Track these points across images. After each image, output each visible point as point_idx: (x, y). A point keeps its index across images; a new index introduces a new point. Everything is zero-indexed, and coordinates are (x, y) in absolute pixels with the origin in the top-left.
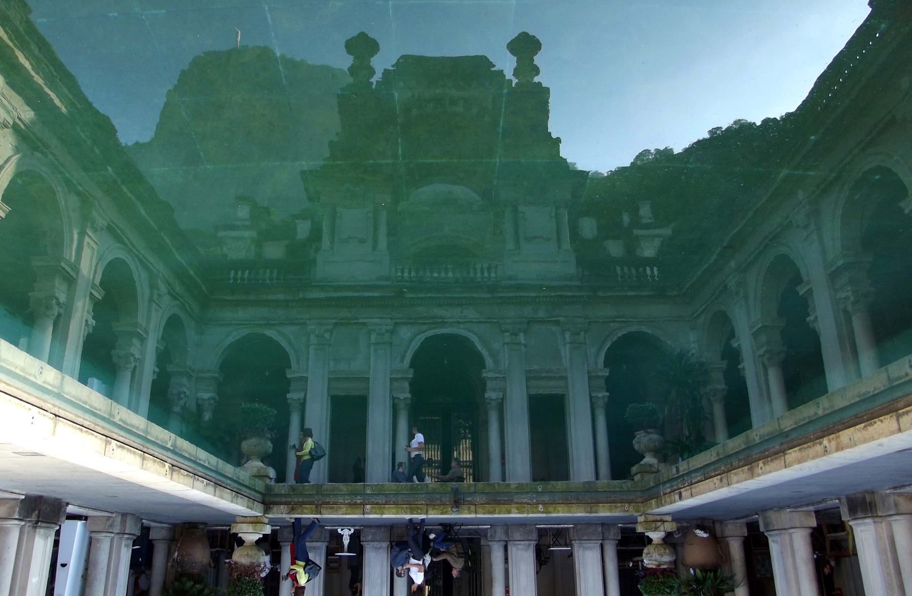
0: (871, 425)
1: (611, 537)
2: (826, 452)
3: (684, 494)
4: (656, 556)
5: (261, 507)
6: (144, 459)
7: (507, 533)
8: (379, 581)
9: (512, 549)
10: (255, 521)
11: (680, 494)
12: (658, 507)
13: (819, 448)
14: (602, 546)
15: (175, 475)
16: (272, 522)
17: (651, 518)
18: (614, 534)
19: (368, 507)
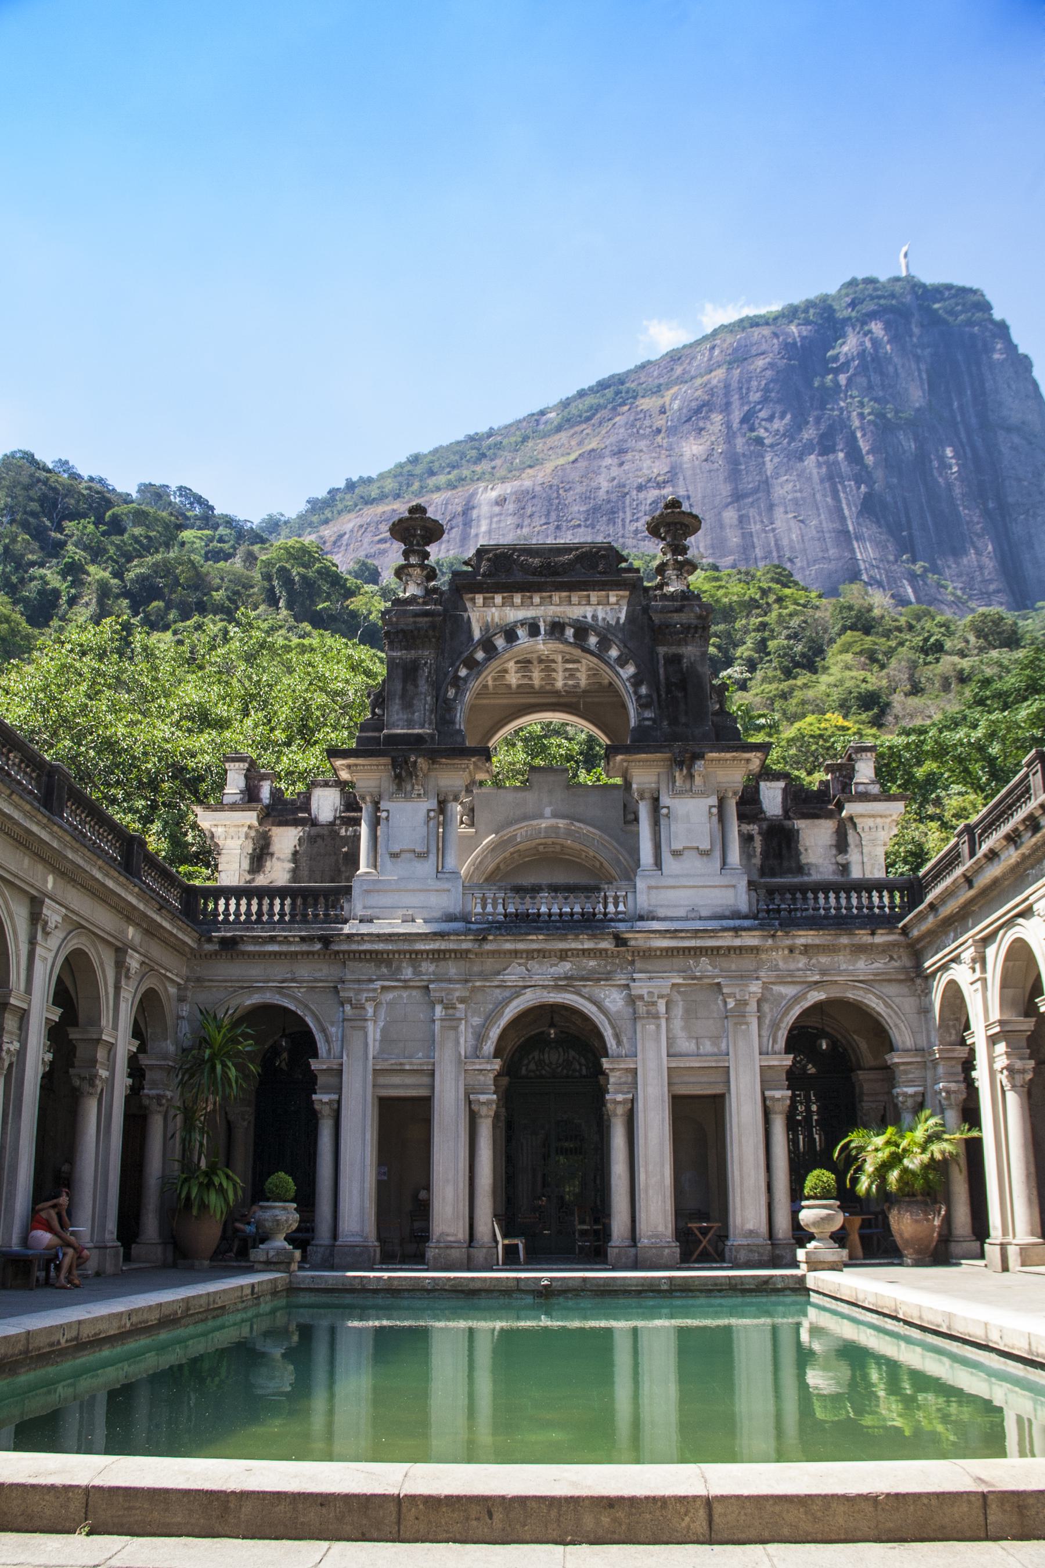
0: (95, 1334)
1: (321, 1250)
2: (130, 1314)
3: (249, 1291)
4: (282, 1216)
5: (810, 1283)
6: (920, 1318)
7: (469, 1257)
8: (651, 1192)
9: (462, 1234)
10: (814, 1265)
11: (253, 1293)
12: (276, 1279)
13: (134, 1319)
14: (335, 1236)
15: (893, 1304)
16: (795, 1265)
17: (282, 1267)
18: (317, 1253)
19: (665, 1287)
